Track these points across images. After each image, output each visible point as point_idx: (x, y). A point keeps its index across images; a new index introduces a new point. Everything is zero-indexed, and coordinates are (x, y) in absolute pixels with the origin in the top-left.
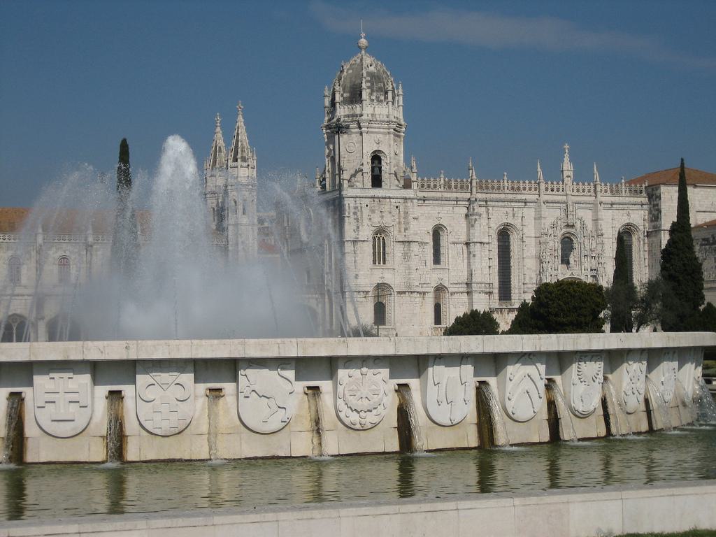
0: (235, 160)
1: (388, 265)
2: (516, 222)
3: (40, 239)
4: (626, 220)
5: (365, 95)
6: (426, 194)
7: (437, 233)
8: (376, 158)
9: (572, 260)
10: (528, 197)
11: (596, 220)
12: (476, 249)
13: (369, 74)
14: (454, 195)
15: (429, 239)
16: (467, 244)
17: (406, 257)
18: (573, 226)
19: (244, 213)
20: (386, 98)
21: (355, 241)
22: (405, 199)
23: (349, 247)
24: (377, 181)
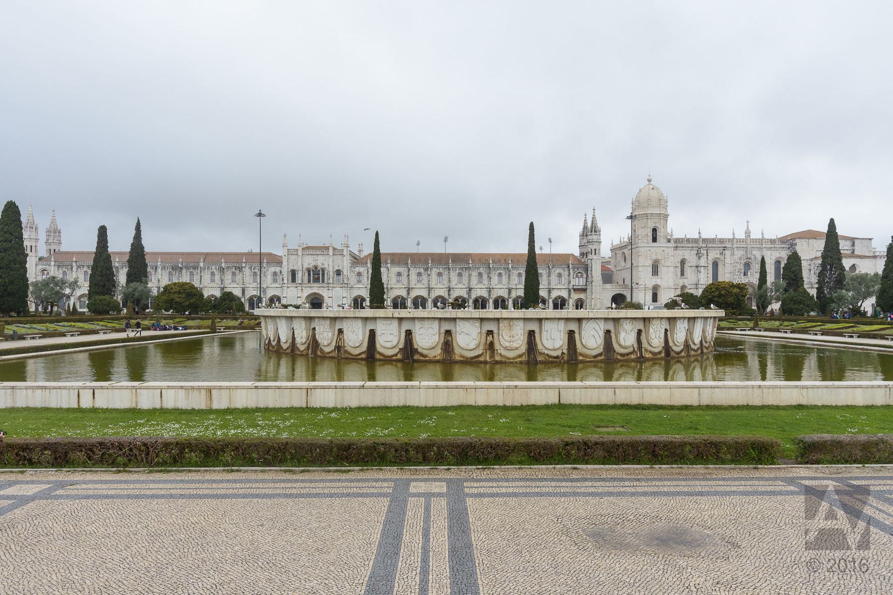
0: (592, 232)
1: (659, 276)
3: (510, 266)
4: (778, 255)
6: (679, 245)
7: (683, 262)
9: (749, 274)
10: (728, 246)
12: (702, 269)
14: (691, 245)
15: (679, 265)
16: (697, 267)
24: (654, 240)
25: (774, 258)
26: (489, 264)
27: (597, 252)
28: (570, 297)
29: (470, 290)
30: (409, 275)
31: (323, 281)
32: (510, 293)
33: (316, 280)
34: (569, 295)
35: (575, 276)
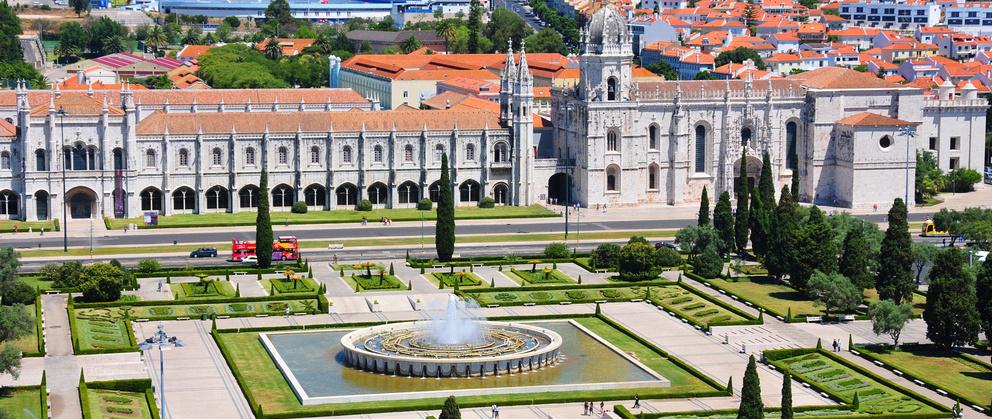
0: (519, 80)
2: (709, 119)
5: (604, 41)
8: (612, 81)
10: (718, 103)
11: (766, 117)
12: (681, 141)
13: (610, 24)
17: (629, 145)
18: (751, 121)
19: (524, 114)
20: (619, 40)
21: (595, 138)
22: (630, 109)
23: (590, 142)
24: (611, 96)
25: (784, 120)
26: (361, 134)
27: (527, 111)
28: (484, 184)
29: (330, 175)
30: (231, 153)
31: (92, 167)
32: (392, 176)
33: (80, 166)
34: (484, 176)
35: (493, 149)
